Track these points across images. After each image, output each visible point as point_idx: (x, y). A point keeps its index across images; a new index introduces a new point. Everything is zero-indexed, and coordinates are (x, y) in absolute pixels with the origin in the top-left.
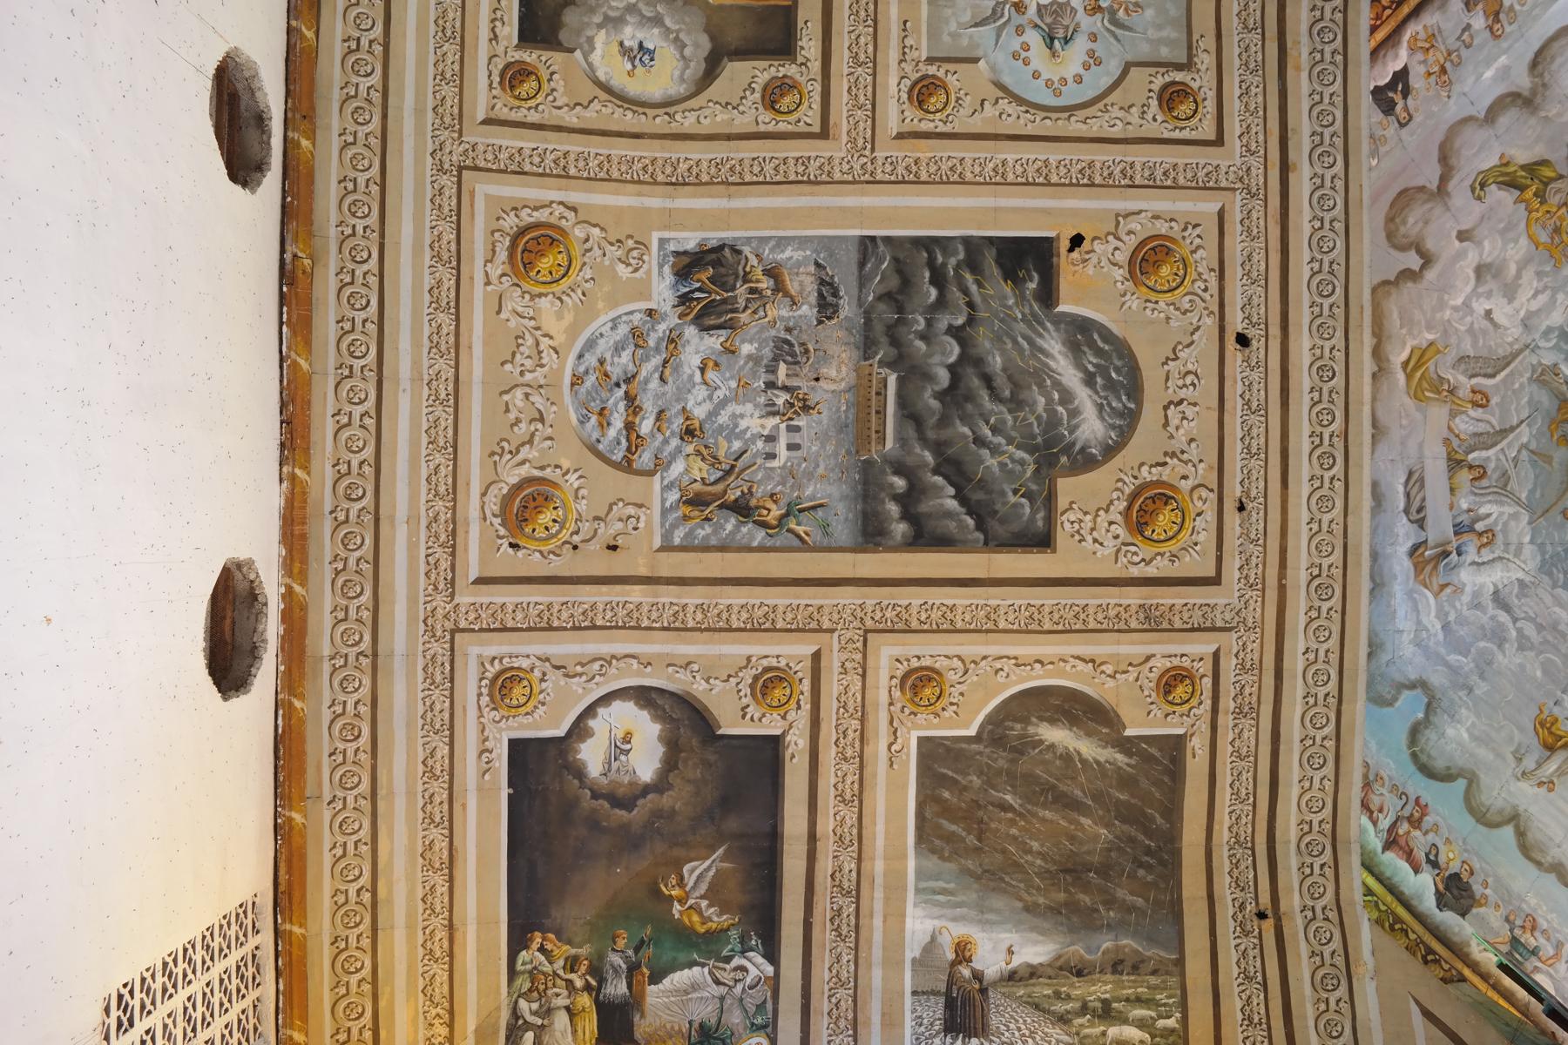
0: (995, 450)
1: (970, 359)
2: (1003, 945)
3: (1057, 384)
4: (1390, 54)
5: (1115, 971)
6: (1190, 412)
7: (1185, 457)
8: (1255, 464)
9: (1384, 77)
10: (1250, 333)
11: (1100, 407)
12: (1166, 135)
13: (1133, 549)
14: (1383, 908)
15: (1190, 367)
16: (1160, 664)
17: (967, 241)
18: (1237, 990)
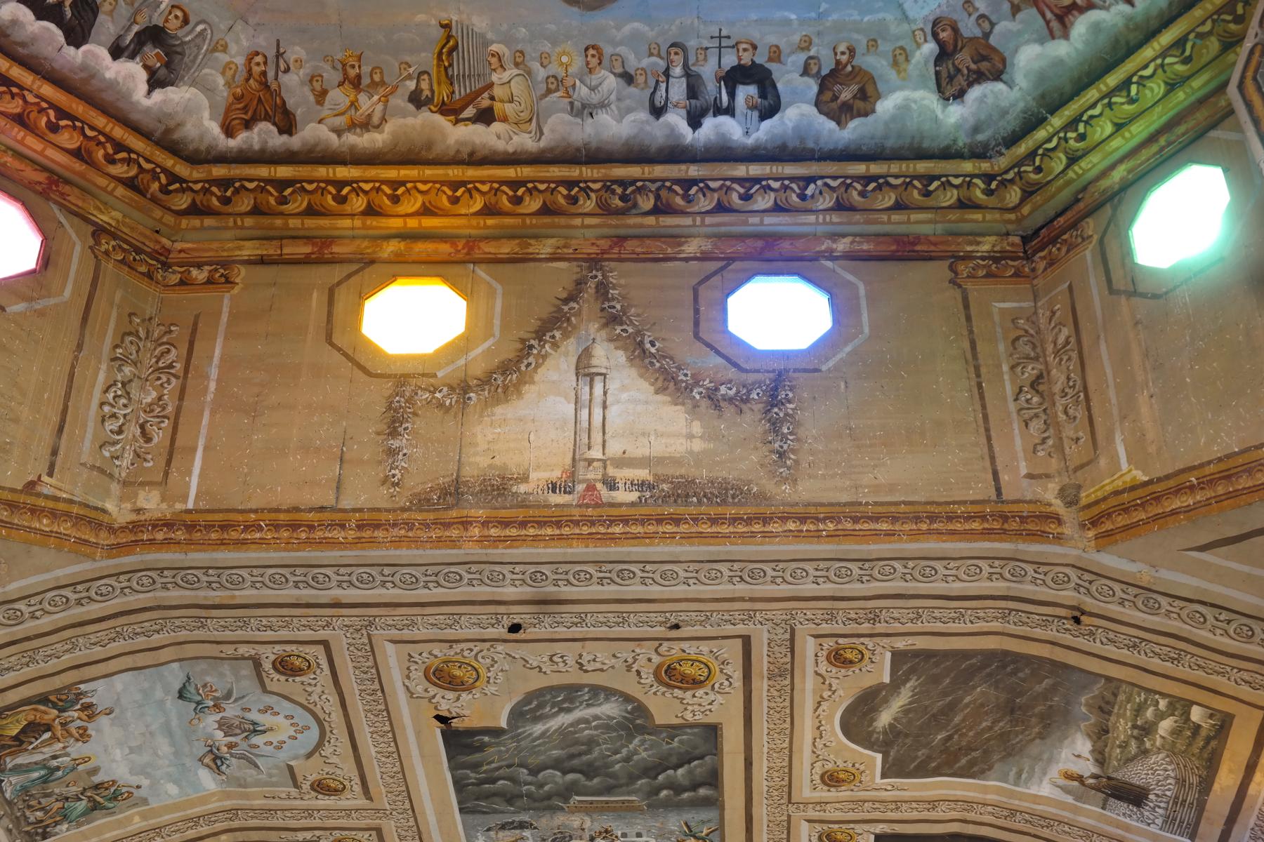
0: (636, 752)
1: (557, 765)
2: (1076, 753)
3: (571, 725)
4: (18, 35)
5: (1110, 713)
6: (586, 657)
7: (630, 660)
8: (632, 619)
9: (48, 29)
10: (507, 622)
11: (588, 706)
12: (327, 671)
13: (717, 686)
14: (1207, 27)
15: (546, 659)
16: (823, 667)
17: (453, 769)
18: (1143, 656)
